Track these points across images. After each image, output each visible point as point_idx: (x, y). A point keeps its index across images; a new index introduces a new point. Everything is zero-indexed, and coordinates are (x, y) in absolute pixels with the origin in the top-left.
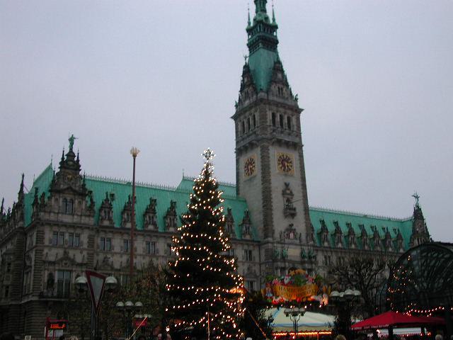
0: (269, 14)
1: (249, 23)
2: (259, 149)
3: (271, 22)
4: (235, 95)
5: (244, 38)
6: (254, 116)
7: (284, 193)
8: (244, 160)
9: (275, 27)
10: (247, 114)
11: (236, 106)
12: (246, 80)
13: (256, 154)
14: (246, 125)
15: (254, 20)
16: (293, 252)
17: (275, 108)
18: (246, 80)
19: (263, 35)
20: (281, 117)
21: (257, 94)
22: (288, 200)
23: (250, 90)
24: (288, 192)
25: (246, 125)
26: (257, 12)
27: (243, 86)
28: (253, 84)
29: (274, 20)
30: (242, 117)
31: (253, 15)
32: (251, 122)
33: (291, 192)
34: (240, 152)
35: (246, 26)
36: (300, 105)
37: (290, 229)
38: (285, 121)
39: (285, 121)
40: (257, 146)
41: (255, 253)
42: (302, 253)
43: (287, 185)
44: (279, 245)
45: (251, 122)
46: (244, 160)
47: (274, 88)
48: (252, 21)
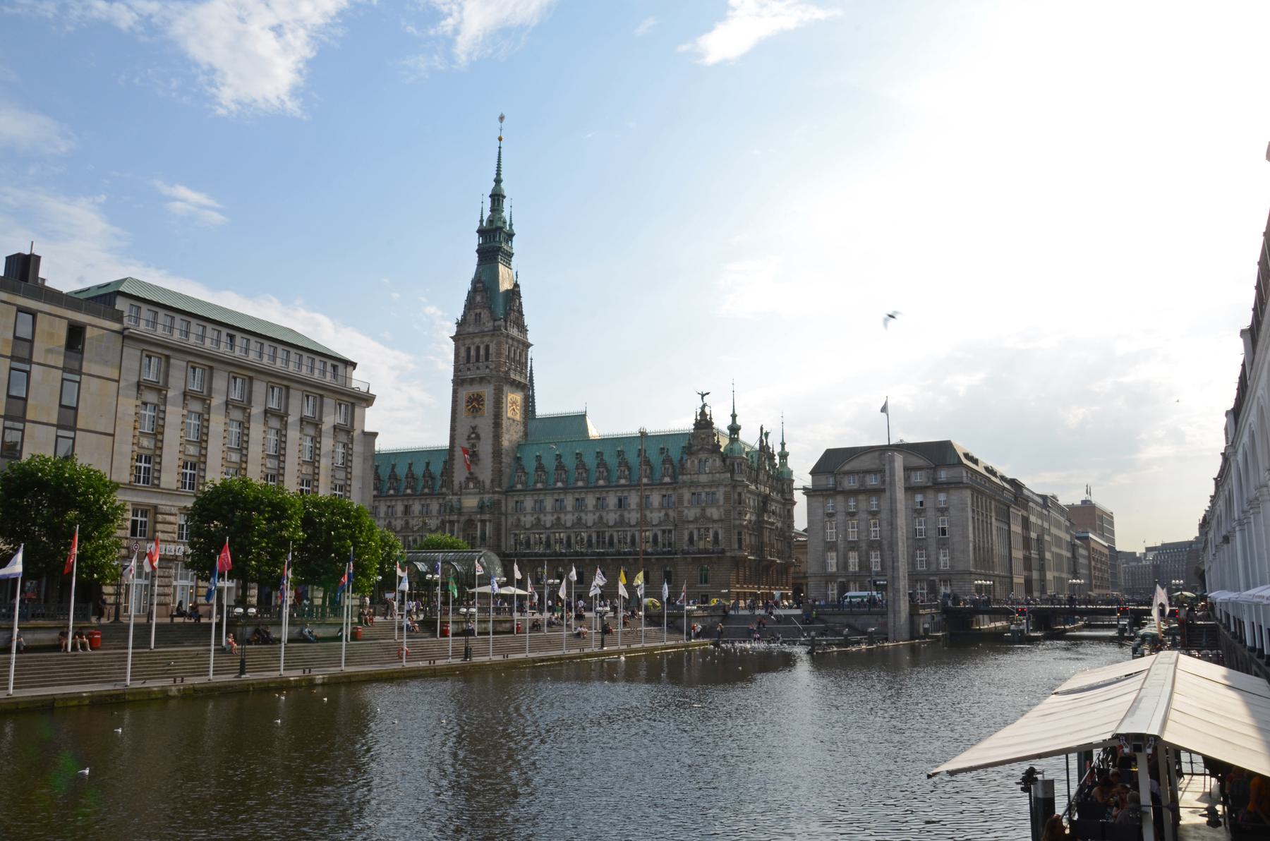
0: (506, 214)
1: (481, 221)
2: (492, 387)
4: (459, 313)
5: (474, 241)
6: (487, 348)
8: (465, 393)
9: (510, 236)
10: (477, 340)
11: (459, 325)
12: (478, 298)
13: (487, 391)
14: (473, 353)
15: (491, 221)
17: (510, 341)
18: (478, 298)
19: (494, 242)
21: (495, 320)
23: (485, 315)
25: (473, 353)
26: (492, 210)
27: (470, 304)
28: (490, 308)
29: (511, 225)
30: (468, 342)
31: (487, 214)
32: (482, 352)
34: (458, 382)
36: (531, 338)
40: (489, 382)
45: (482, 352)
46: (465, 393)
47: (513, 316)
48: (485, 218)
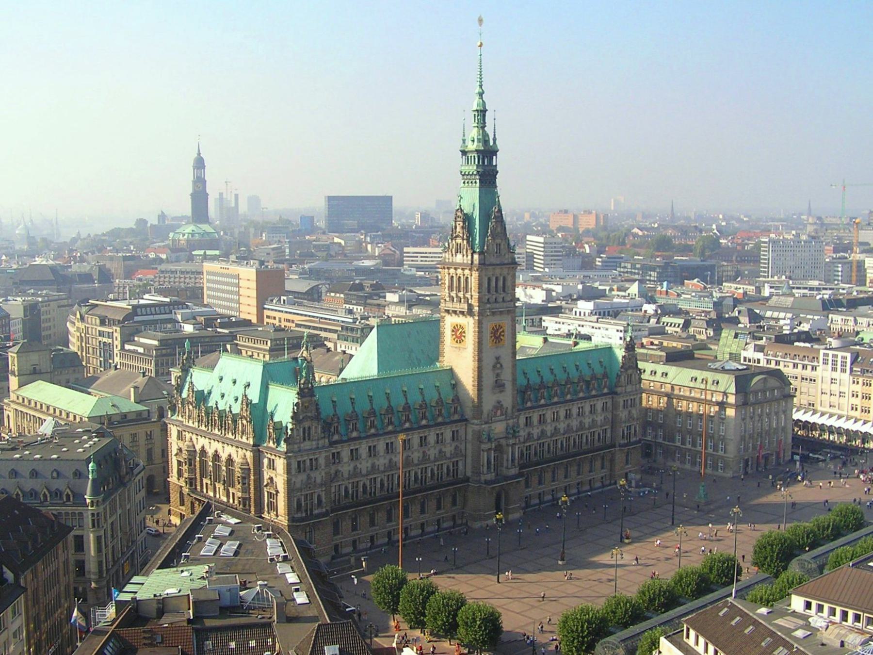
3: (491, 143)
7: (494, 367)
16: (499, 428)
20: (497, 279)
22: (498, 375)
24: (498, 366)
29: (495, 140)
33: (501, 366)
35: (459, 146)
37: (499, 406)
38: (501, 283)
39: (501, 283)
41: (462, 433)
42: (507, 429)
43: (498, 358)
44: (487, 426)
